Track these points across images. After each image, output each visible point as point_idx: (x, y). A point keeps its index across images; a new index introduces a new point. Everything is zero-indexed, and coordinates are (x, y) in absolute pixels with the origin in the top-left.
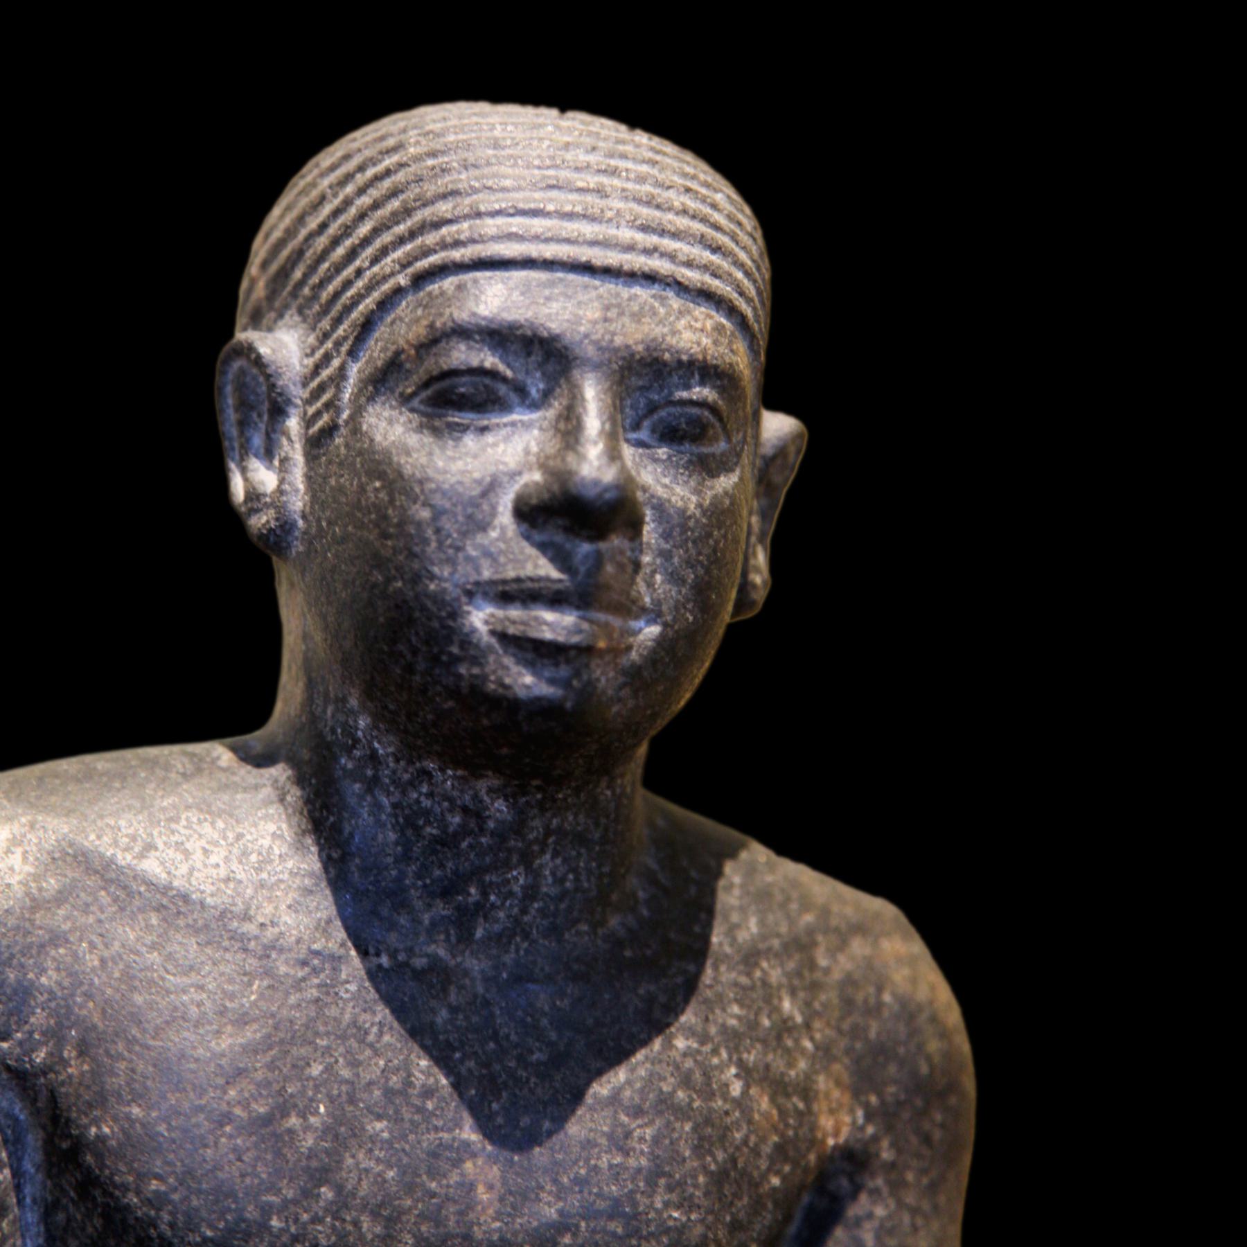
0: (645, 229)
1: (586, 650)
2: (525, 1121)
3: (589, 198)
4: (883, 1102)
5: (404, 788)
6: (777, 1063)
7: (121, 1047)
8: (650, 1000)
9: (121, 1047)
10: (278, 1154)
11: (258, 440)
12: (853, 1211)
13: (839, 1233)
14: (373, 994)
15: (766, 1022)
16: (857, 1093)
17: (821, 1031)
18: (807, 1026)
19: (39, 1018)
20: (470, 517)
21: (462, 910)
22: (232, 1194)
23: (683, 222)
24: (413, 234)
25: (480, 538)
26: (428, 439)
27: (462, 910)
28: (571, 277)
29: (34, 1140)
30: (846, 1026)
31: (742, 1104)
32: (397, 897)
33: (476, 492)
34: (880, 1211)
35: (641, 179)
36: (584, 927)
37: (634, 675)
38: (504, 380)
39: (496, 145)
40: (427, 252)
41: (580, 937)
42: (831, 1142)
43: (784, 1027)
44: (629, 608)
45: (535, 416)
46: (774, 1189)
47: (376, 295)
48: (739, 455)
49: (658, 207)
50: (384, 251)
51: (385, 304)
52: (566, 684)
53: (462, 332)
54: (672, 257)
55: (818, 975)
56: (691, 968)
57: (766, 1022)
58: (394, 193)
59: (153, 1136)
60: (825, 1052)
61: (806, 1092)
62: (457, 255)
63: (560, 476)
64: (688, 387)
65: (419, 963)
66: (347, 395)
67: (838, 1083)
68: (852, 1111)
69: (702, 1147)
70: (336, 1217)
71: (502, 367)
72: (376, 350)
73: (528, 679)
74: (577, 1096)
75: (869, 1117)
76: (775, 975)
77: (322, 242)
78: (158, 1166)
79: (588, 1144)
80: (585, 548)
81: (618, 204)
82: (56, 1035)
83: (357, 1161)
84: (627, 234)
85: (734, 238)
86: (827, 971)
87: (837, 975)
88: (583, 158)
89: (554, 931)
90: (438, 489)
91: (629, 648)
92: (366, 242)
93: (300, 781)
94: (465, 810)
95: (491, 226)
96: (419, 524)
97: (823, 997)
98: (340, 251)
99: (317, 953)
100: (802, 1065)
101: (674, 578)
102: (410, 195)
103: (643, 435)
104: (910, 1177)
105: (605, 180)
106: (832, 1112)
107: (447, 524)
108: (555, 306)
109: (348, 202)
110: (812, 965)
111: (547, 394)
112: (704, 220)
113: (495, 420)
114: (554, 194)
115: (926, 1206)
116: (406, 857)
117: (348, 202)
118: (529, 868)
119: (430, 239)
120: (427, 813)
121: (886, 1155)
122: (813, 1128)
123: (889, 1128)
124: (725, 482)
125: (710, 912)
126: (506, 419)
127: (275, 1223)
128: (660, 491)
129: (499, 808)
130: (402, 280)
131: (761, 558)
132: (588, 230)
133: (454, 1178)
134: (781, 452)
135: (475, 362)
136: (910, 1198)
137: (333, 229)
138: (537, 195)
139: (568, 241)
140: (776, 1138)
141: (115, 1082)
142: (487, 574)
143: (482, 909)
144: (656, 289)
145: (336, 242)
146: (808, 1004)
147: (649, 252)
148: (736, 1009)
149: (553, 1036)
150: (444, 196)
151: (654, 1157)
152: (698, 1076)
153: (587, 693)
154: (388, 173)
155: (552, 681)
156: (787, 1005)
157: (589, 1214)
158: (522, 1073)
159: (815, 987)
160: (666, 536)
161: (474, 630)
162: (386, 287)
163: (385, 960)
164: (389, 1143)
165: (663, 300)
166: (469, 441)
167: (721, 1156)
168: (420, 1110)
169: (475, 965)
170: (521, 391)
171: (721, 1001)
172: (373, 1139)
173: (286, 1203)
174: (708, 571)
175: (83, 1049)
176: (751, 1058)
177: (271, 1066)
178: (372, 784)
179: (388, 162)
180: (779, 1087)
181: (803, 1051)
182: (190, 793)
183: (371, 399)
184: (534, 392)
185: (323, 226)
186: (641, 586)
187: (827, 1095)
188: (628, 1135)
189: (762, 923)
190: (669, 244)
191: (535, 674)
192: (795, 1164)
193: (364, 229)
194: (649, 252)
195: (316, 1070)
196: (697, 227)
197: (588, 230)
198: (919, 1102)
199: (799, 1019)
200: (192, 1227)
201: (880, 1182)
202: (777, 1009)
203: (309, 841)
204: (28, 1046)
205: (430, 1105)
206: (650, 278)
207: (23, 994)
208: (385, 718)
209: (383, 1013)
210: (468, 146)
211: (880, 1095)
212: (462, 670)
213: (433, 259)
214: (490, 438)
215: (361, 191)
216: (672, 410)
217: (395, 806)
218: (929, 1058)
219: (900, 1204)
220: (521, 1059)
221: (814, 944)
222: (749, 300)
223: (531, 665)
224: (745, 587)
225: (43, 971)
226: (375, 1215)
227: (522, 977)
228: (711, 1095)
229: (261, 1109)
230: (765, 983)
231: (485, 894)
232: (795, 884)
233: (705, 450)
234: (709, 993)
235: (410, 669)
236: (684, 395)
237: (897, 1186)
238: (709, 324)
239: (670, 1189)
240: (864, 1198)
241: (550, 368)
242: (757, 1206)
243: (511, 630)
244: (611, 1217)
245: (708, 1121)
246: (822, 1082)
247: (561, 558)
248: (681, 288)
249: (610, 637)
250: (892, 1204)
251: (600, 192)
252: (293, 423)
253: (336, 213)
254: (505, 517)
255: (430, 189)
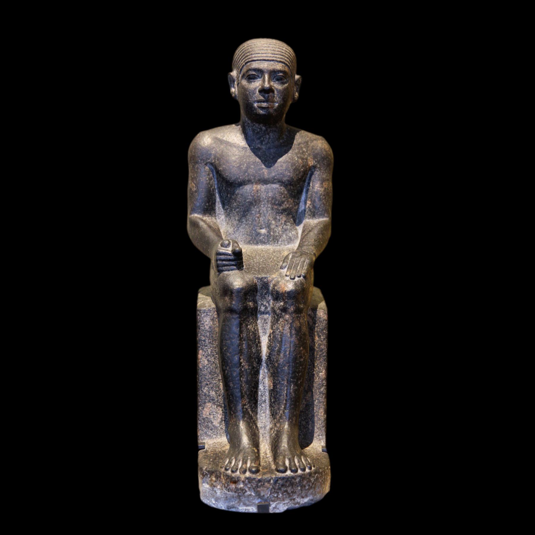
0: (272, 54)
1: (268, 108)
2: (270, 165)
3: (265, 51)
4: (317, 160)
5: (252, 127)
6: (302, 156)
7: (222, 159)
8: (285, 150)
9: (222, 159)
10: (241, 170)
11: (232, 85)
12: (315, 173)
13: (313, 176)
14: (251, 151)
15: (301, 151)
16: (314, 159)
17: (309, 152)
18: (307, 152)
19: (213, 157)
20: (253, 93)
21: (261, 141)
22: (235, 175)
23: (278, 53)
24: (245, 58)
25: (255, 95)
26: (248, 83)
27: (261, 141)
28: (263, 61)
29: (214, 171)
30: (312, 151)
31: (297, 161)
32: (253, 140)
33: (254, 89)
34: (318, 173)
35: (272, 47)
36: (277, 142)
37: (275, 110)
38: (256, 75)
39: (255, 45)
40: (246, 60)
41: (276, 143)
42: (310, 165)
43: (304, 152)
44: (273, 102)
45: (260, 79)
46: (302, 171)
47: (242, 66)
48: (288, 81)
49: (274, 51)
50: (242, 60)
51: (243, 67)
52: (266, 112)
53: (250, 70)
54: (276, 57)
55: (309, 145)
56: (291, 146)
57: (301, 151)
58: (243, 52)
59: (226, 169)
60: (309, 155)
61: (307, 159)
62: (249, 60)
63: (263, 86)
64: (279, 74)
65: (256, 147)
66: (240, 79)
67: (311, 158)
68: (313, 161)
69: (292, 166)
70: (248, 176)
71: (255, 74)
72: (242, 73)
73: (262, 112)
74: (276, 161)
75: (316, 162)
76: (303, 146)
77: (237, 59)
78: (227, 172)
79: (278, 167)
80: (267, 95)
81: (269, 51)
82: (215, 159)
83: (250, 170)
84: (270, 55)
85: (285, 53)
86: (310, 145)
87: (311, 145)
88: (265, 45)
89: (273, 142)
90: (249, 90)
91: (274, 107)
92: (240, 59)
93: (241, 127)
94: (260, 129)
95: (253, 56)
96: (248, 94)
97: (309, 148)
98: (238, 60)
99: (244, 147)
100: (306, 156)
101: (279, 98)
102: (245, 53)
103: (274, 80)
104: (322, 169)
105: (268, 48)
106: (310, 161)
107: (251, 94)
108: (261, 65)
109: (239, 54)
110: (308, 144)
111: (261, 76)
112: (281, 52)
113: (256, 80)
114: (261, 51)
115: (324, 172)
116: (254, 135)
117: (239, 54)
118: (269, 135)
119: (247, 58)
120: (255, 129)
121: (318, 166)
122: (308, 163)
123: (319, 163)
124: (286, 85)
125: (294, 139)
126: (257, 80)
127: (241, 177)
128: (277, 87)
129: (264, 128)
130: (244, 64)
131: (297, 94)
132: (265, 55)
133: (262, 172)
134: (298, 80)
135: (252, 73)
136: (322, 171)
137: (238, 58)
138: (259, 51)
139: (262, 57)
140: (302, 165)
141: (222, 163)
142: (256, 99)
143: (263, 140)
144: (274, 62)
145: (238, 59)
146: (307, 149)
147: (273, 57)
148: (297, 150)
149: (273, 155)
150: (248, 52)
151: (286, 167)
152: (291, 158)
153: (269, 112)
154: (243, 50)
155: (264, 112)
156: (304, 149)
157: (278, 174)
158: (269, 159)
159: (308, 147)
160: (278, 93)
161: (255, 106)
162: (243, 65)
163: (252, 147)
164: (254, 168)
165: (275, 63)
166: (253, 83)
167: (294, 167)
168: (257, 164)
169: (264, 147)
170: (258, 76)
171: (295, 149)
172: (252, 168)
173: (242, 175)
174: (284, 96)
175: (218, 160)
176: (298, 156)
177: (239, 160)
178: (249, 127)
179: (243, 48)
180: (302, 159)
181: (306, 155)
182: (229, 130)
183: (242, 79)
184: (260, 76)
185: (237, 57)
186: (275, 99)
187: (310, 160)
188: (282, 165)
189: (301, 140)
190: (276, 56)
191: (262, 111)
192: (305, 167)
193: (240, 57)
194: (273, 57)
195: (244, 160)
196: (280, 53)
197: (265, 55)
198: (322, 160)
199: (306, 151)
200: (231, 178)
201: (318, 169)
202: (303, 150)
203: (243, 134)
204: (212, 160)
205: (258, 164)
206: (273, 60)
207: (211, 154)
208: (248, 118)
209: (252, 154)
210: (251, 45)
211: (317, 159)
212: (254, 111)
213: (247, 61)
214: (255, 83)
215: (240, 52)
216: (277, 77)
217: (252, 129)
218: (324, 154)
219: (321, 172)
220: (270, 158)
221: (308, 142)
222: (287, 61)
223: (262, 110)
224: (294, 98)
225: (213, 151)
226: (253, 176)
227: (269, 148)
228: (293, 160)
229: (238, 165)
230: (301, 147)
231: (264, 138)
232: (307, 135)
233: (283, 81)
234: (293, 148)
235: (249, 112)
236: (278, 75)
237: (320, 170)
238: (281, 65)
239: (288, 171)
240: (316, 171)
241: (262, 73)
242: (300, 172)
243: (259, 106)
244: (281, 175)
245: (293, 163)
246: (309, 158)
247: (264, 97)
248: (277, 61)
249: (271, 106)
250: (320, 172)
251: (267, 50)
252: (236, 83)
253: (238, 55)
254: (257, 92)
255: (247, 52)
